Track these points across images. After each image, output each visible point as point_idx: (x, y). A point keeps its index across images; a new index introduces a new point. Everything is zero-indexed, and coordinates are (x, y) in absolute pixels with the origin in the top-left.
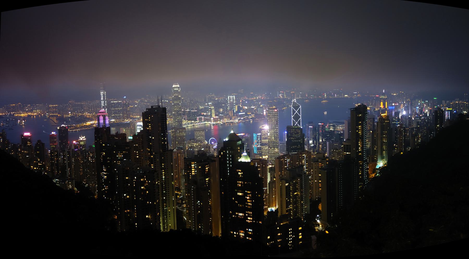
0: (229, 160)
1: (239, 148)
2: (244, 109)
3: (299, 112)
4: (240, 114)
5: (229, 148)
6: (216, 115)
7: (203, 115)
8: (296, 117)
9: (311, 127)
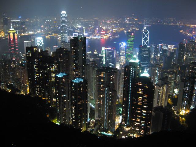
0: (132, 74)
1: (138, 67)
2: (103, 29)
3: (147, 36)
4: (102, 32)
5: (133, 66)
6: (86, 33)
7: (77, 32)
8: (145, 39)
9: (154, 46)
